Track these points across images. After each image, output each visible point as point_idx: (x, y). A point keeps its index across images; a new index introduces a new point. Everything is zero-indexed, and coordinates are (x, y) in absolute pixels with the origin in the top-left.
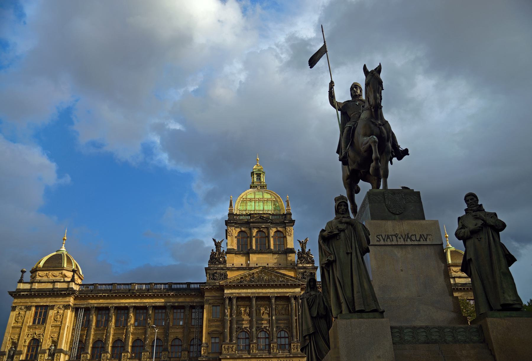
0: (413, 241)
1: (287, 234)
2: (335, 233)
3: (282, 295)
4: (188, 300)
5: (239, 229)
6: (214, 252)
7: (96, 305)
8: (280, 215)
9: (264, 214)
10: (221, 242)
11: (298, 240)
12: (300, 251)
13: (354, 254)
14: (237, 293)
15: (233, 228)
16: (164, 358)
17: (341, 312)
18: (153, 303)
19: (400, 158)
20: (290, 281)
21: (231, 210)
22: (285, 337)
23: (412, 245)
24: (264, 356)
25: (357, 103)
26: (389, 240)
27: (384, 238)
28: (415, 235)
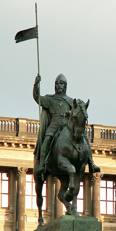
25: (61, 104)
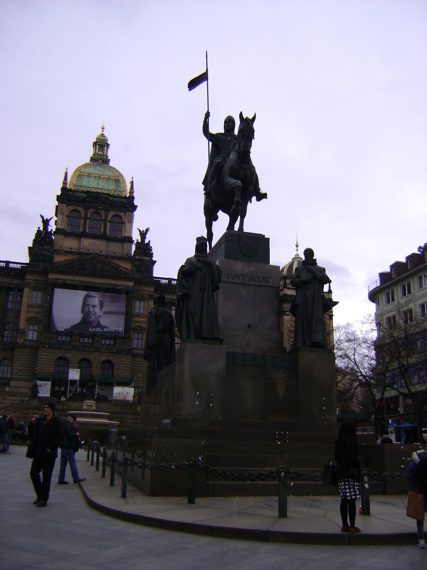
0: (256, 281)
1: (127, 220)
2: (193, 270)
5: (73, 207)
6: (41, 230)
8: (121, 197)
9: (103, 193)
10: (50, 219)
11: (138, 229)
12: (139, 241)
13: (206, 291)
14: (63, 280)
15: (65, 205)
17: (189, 337)
19: (258, 199)
20: (124, 273)
21: (65, 183)
23: (255, 285)
24: (86, 349)
26: (236, 278)
27: (233, 276)
28: (259, 277)
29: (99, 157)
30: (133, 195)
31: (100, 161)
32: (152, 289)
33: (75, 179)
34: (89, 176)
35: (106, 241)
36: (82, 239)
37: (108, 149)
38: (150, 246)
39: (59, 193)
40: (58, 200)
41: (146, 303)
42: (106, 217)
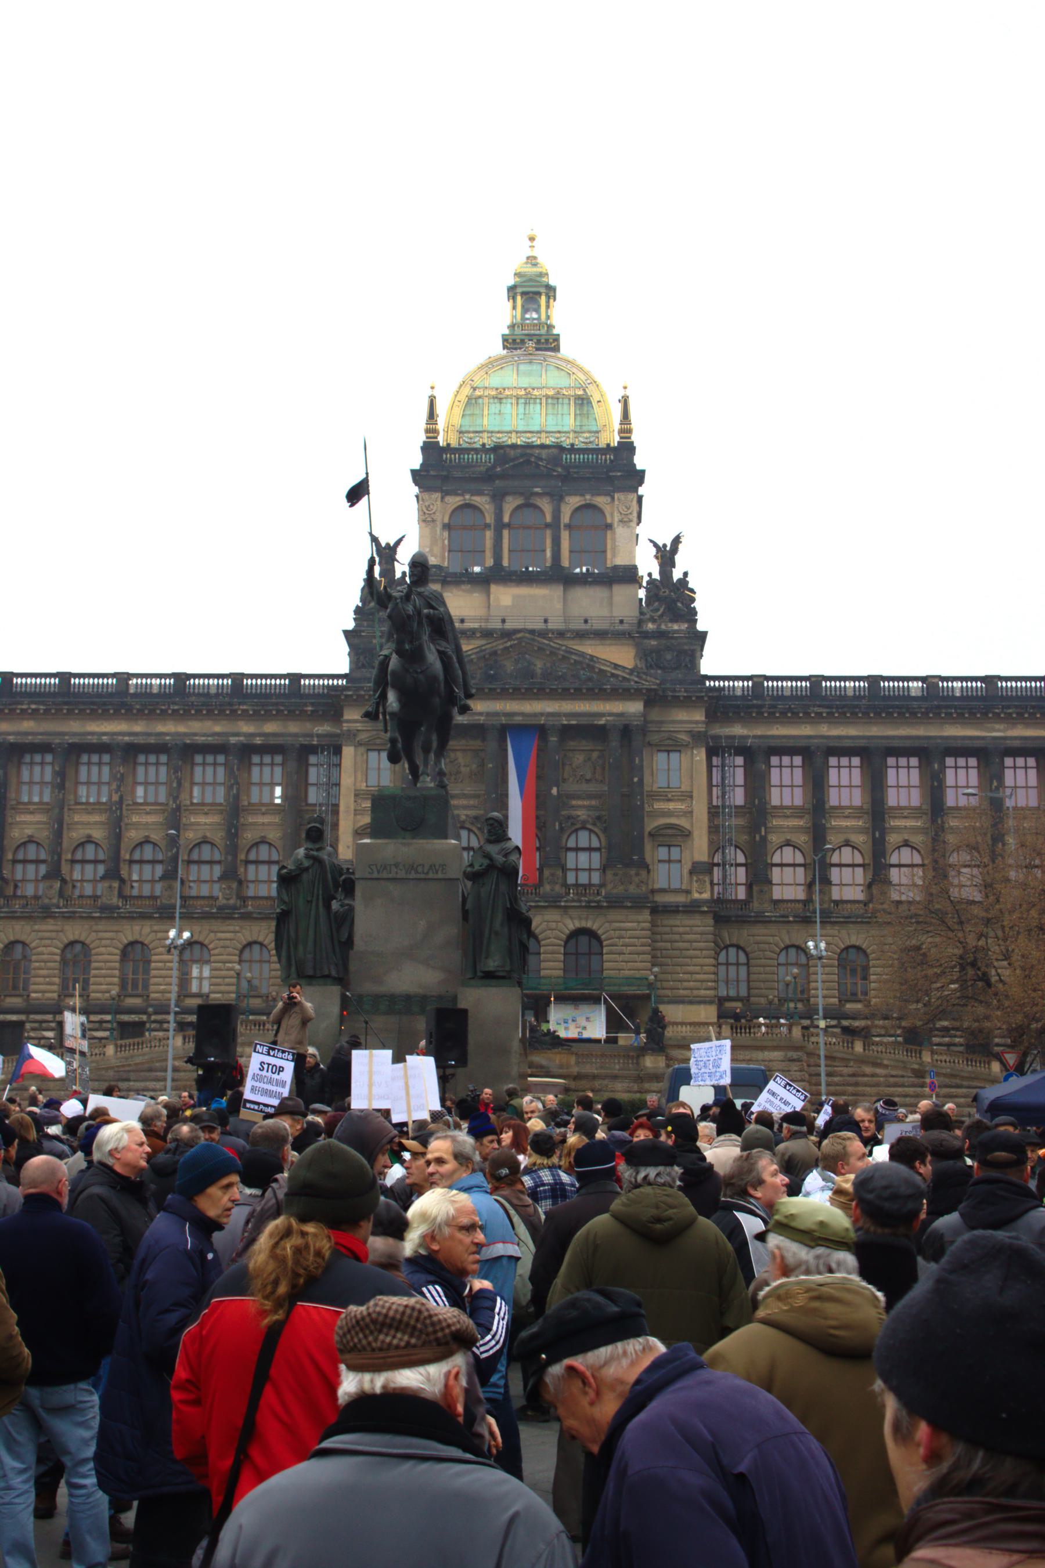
1: (617, 517)
3: (584, 721)
4: (293, 728)
7: (11, 739)
8: (597, 451)
9: (543, 446)
10: (398, 542)
11: (651, 541)
13: (314, 904)
16: (228, 899)
18: (185, 734)
21: (431, 432)
22: (590, 849)
29: (526, 332)
30: (629, 438)
31: (531, 344)
32: (699, 716)
33: (458, 411)
34: (499, 397)
35: (562, 588)
36: (494, 588)
37: (551, 301)
38: (690, 586)
39: (416, 461)
40: (416, 481)
41: (685, 758)
42: (557, 514)
